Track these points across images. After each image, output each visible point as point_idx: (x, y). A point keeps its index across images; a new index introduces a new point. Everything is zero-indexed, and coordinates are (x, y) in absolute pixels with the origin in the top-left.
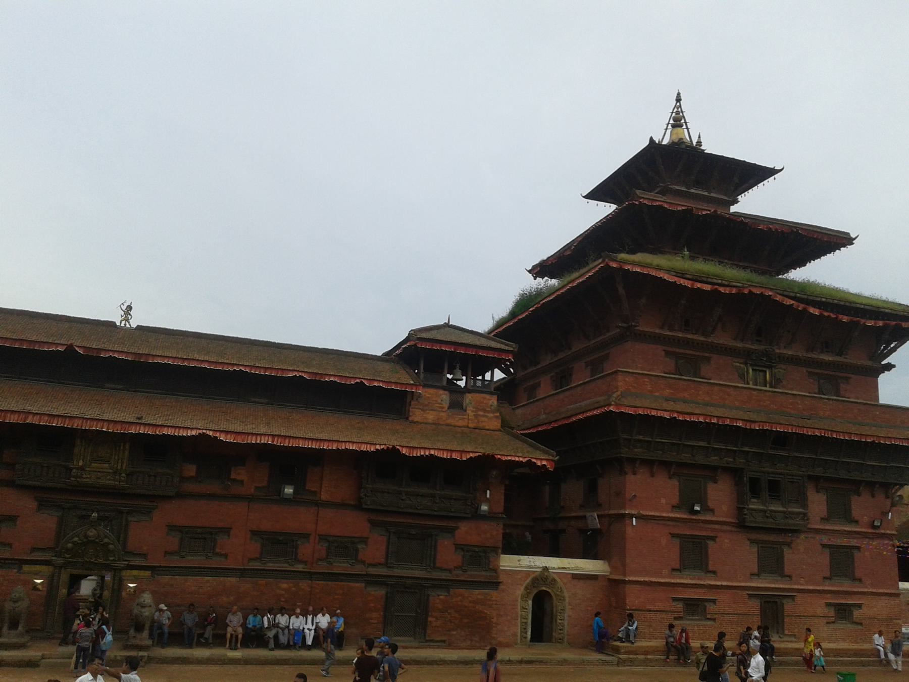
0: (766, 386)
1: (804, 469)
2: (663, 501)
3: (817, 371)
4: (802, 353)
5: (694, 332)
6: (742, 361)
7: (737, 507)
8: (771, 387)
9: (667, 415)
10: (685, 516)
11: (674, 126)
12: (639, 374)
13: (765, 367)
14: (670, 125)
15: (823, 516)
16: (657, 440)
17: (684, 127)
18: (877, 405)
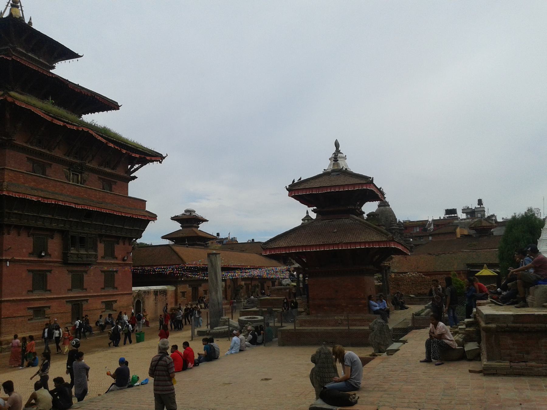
0: (78, 184)
1: (97, 231)
2: (24, 250)
3: (103, 177)
4: (96, 167)
5: (44, 148)
6: (67, 168)
7: (63, 252)
8: (81, 184)
9: (34, 199)
10: (36, 259)
11: (12, 6)
12: (17, 171)
13: (79, 173)
14: (9, 5)
15: (102, 256)
16: (26, 213)
17: (20, 8)
18: (127, 197)
